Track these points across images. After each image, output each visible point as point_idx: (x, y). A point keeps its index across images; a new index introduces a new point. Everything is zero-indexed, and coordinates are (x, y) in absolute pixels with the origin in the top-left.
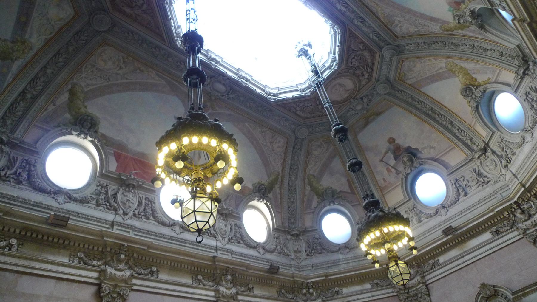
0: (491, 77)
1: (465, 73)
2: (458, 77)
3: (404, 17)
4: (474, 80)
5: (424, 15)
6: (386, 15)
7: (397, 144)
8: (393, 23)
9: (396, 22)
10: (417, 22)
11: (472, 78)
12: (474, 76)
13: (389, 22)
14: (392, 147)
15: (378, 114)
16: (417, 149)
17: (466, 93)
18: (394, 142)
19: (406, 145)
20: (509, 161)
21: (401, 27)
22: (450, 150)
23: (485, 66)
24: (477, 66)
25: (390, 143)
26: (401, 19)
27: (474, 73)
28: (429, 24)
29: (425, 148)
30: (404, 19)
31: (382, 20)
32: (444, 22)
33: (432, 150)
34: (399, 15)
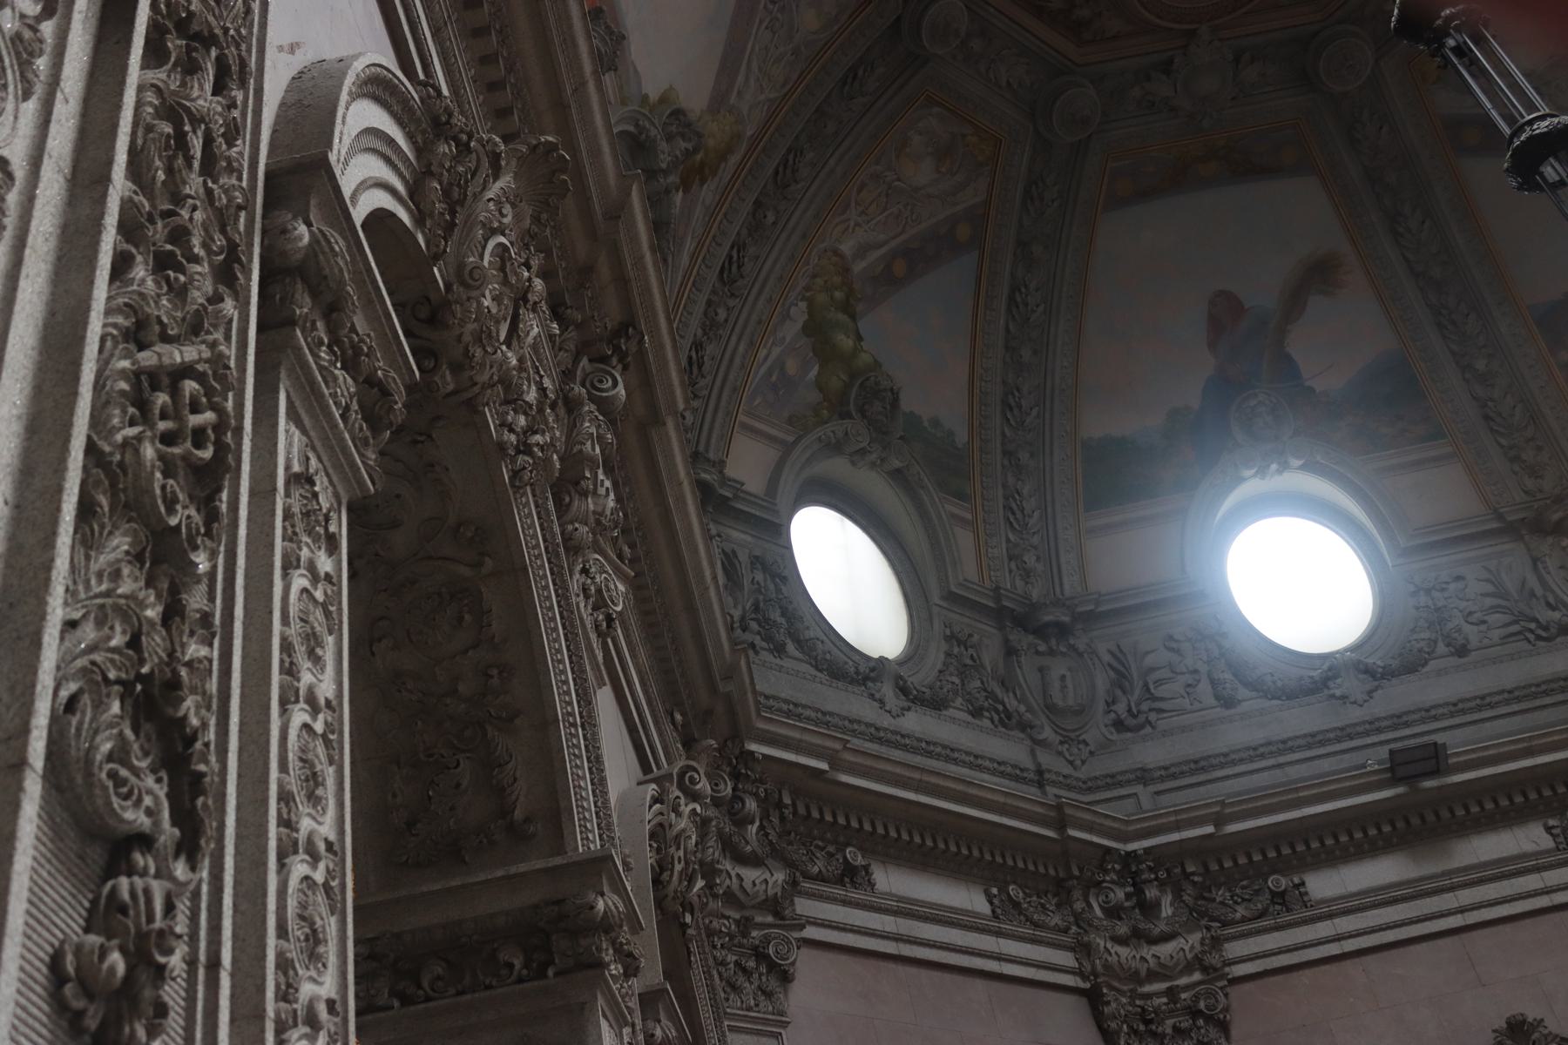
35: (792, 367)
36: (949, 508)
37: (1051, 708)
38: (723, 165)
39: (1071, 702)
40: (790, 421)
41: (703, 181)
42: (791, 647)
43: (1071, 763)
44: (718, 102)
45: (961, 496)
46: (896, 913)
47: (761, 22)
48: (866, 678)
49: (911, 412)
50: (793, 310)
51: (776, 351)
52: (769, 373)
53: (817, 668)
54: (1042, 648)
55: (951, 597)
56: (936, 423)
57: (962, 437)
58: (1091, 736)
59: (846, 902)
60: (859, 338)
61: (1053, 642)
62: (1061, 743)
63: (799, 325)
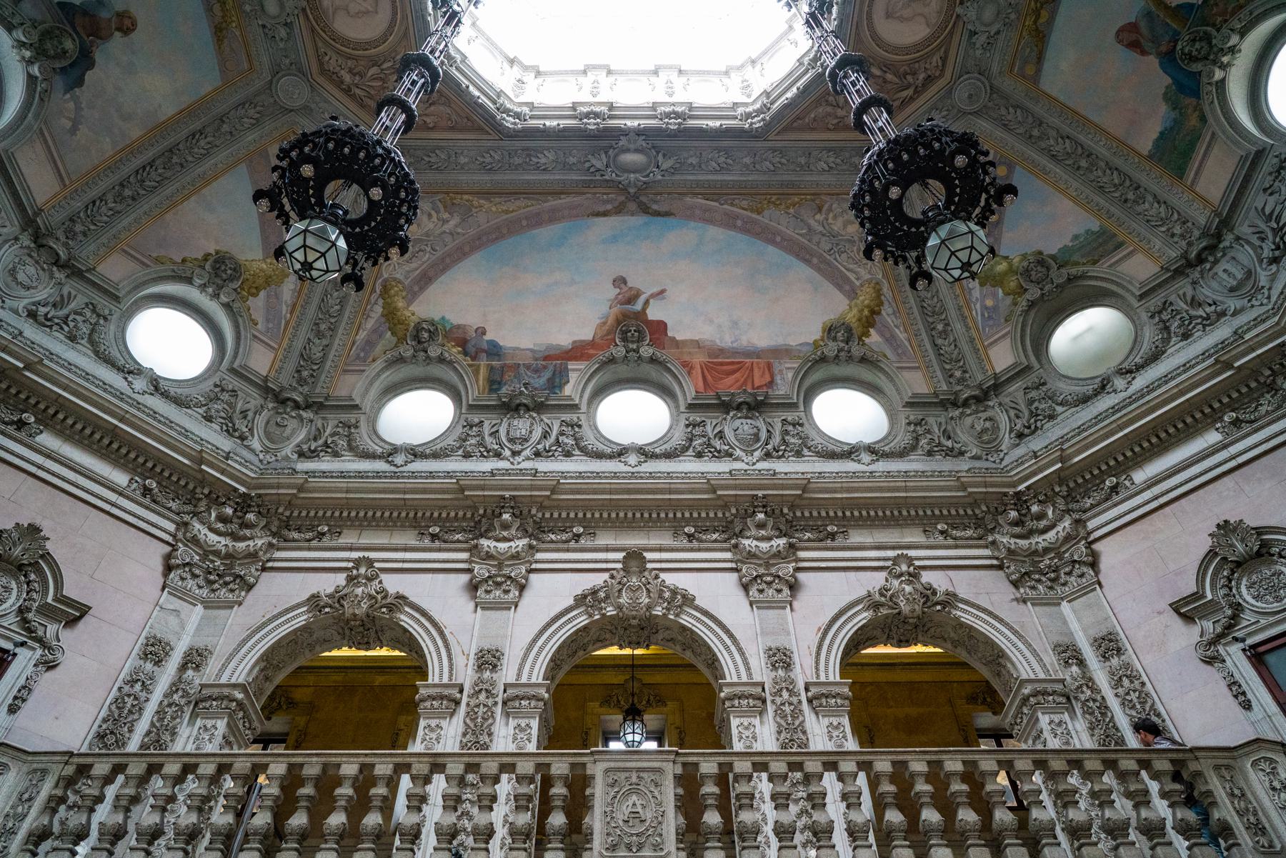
0: (259, 327)
1: (270, 277)
2: (264, 260)
3: (451, 234)
4: (254, 291)
5: (444, 271)
6: (474, 210)
7: (112, 34)
8: (445, 207)
9: (446, 216)
10: (428, 249)
11: (258, 289)
12: (262, 294)
13: (453, 204)
14: (104, 14)
15: (219, 32)
16: (80, 82)
17: (230, 269)
18: (118, 29)
19: (98, 56)
20: (45, 323)
21: (430, 216)
22: (60, 175)
23: (283, 322)
24: (284, 308)
25: (121, 15)
26: (447, 227)
27: (268, 296)
28: (414, 265)
29: (78, 108)
30: (445, 232)
31: (466, 197)
32: (412, 296)
33: (68, 124)
34: (460, 230)
35: (989, 303)
36: (1105, 266)
37: (1232, 290)
38: (883, 297)
39: (1239, 276)
40: (1006, 321)
41: (879, 313)
42: (1059, 409)
43: (1262, 305)
44: (852, 294)
45: (1119, 246)
46: (1149, 487)
47: (835, 259)
48: (1103, 387)
49: (1059, 250)
50: (970, 286)
51: (978, 306)
52: (983, 315)
53: (1075, 406)
54: (1208, 266)
55: (1141, 297)
56: (1076, 237)
57: (1095, 225)
58: (1263, 281)
59: (1115, 505)
60: (1007, 258)
61: (1211, 259)
62: (1249, 301)
63: (978, 285)
